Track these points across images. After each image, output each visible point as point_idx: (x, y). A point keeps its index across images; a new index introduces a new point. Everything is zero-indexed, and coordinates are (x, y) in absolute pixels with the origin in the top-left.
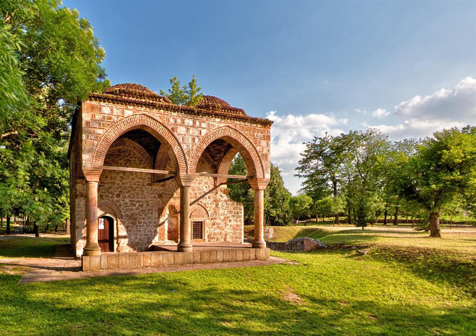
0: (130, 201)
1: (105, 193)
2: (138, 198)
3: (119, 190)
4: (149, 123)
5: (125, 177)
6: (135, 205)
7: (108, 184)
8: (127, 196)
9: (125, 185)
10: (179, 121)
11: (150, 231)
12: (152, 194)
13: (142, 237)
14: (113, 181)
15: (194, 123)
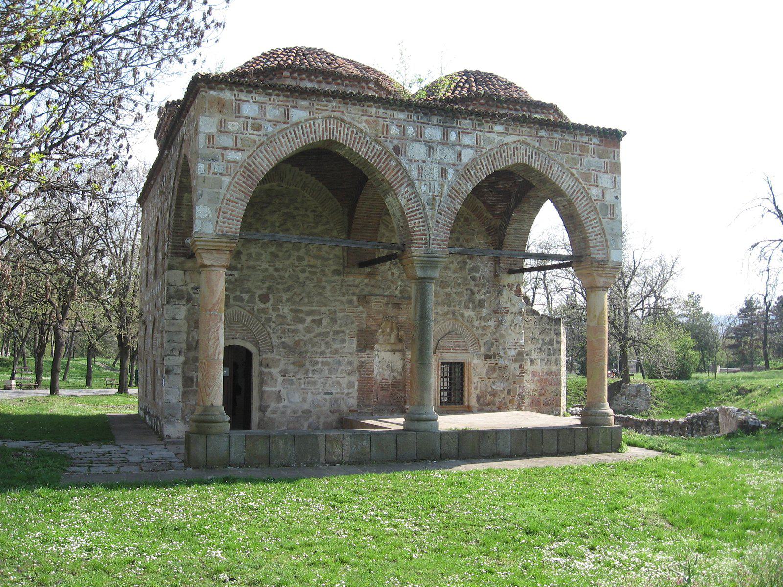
0: (291, 310)
2: (310, 303)
3: (267, 284)
4: (342, 135)
5: (281, 254)
6: (302, 321)
8: (285, 299)
9: (282, 273)
10: (410, 131)
11: (339, 383)
12: (344, 295)
13: (319, 397)
14: (251, 263)
15: (446, 136)
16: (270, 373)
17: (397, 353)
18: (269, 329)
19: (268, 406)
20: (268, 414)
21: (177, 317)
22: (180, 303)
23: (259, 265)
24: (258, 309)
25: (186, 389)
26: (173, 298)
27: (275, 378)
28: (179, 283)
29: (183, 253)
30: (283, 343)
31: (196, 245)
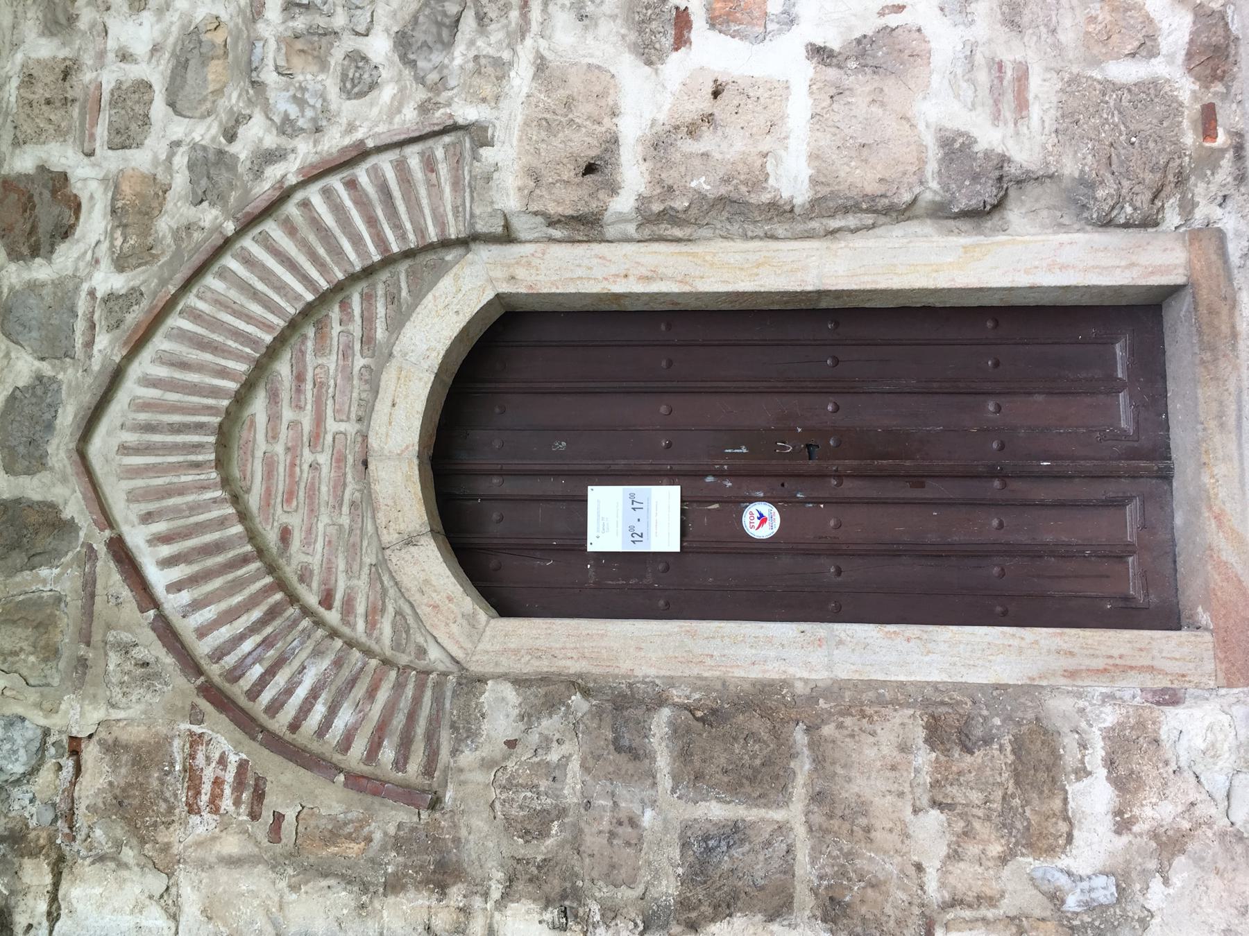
8: (44, 49)
16: (658, 147)
18: (288, 171)
19: (955, 149)
20: (1024, 144)
24: (121, 263)
25: (804, 899)
27: (703, 103)
30: (403, 42)
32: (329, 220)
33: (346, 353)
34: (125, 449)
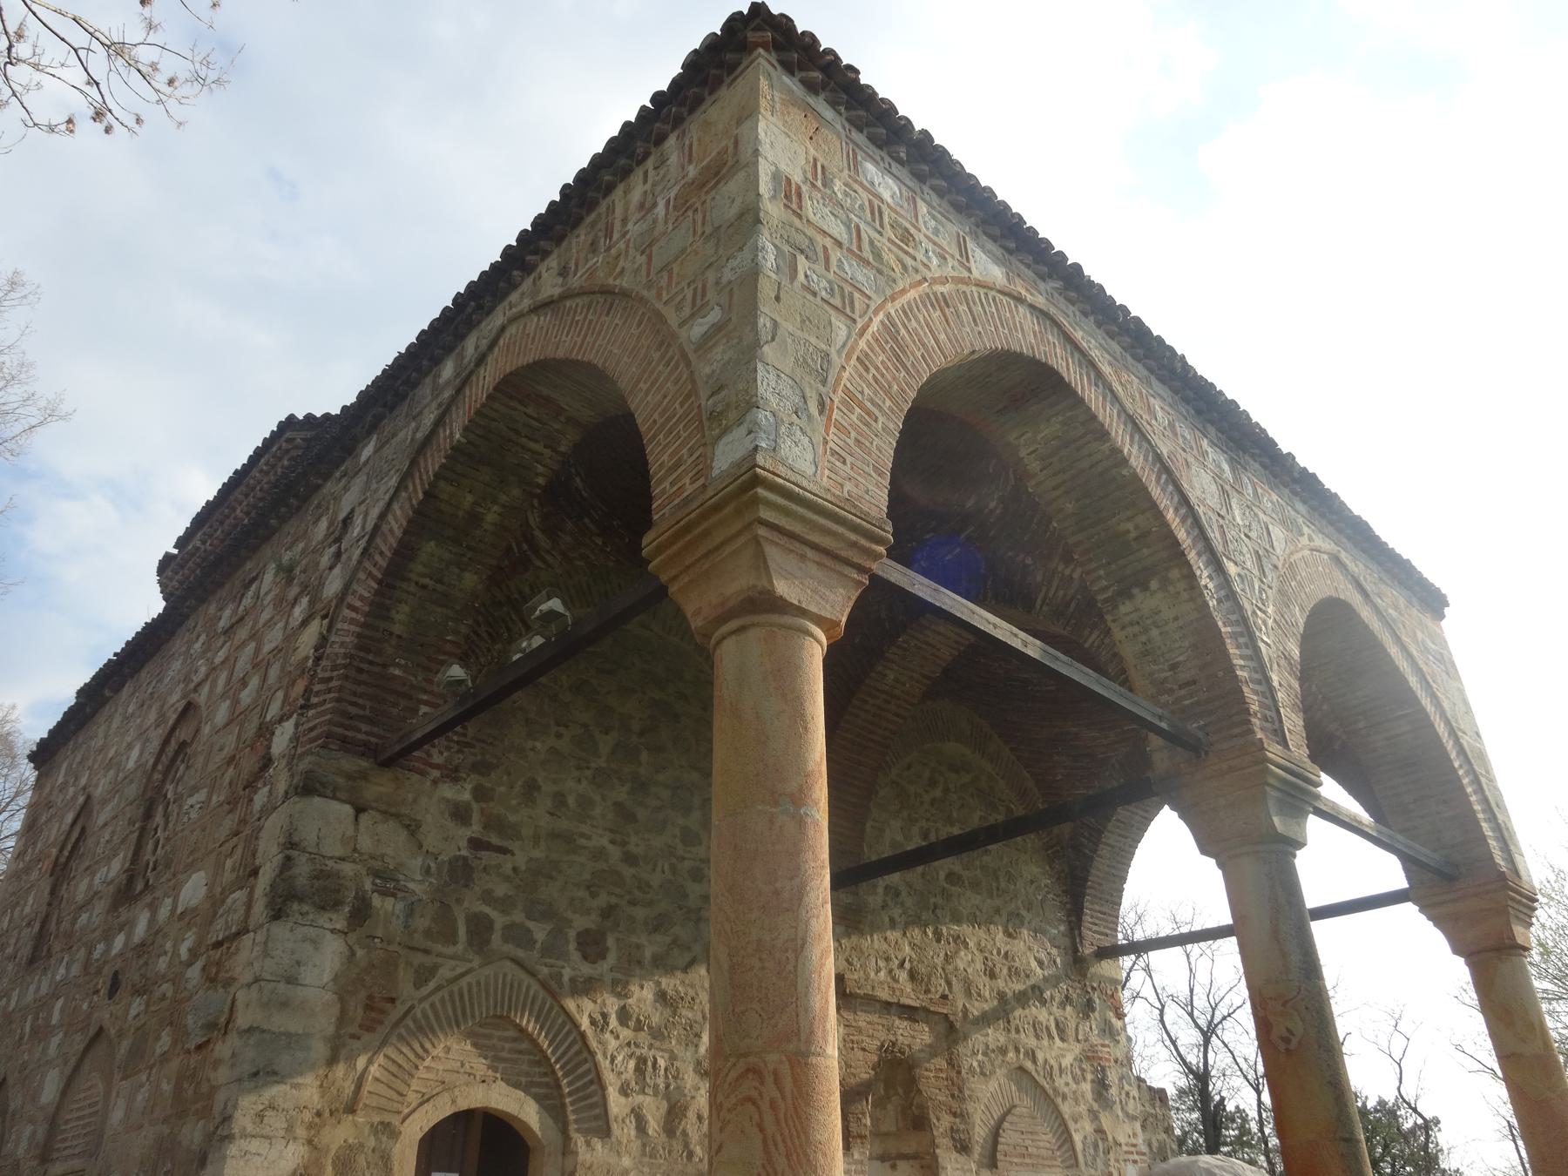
1: (505, 904)
3: (603, 900)
5: (642, 814)
7: (536, 840)
8: (648, 954)
14: (564, 824)
17: (902, 1165)
21: (309, 975)
22: (323, 920)
23: (583, 835)
24: (572, 980)
26: (301, 900)
28: (333, 848)
29: (365, 744)
31: (756, 501)
32: (580, 1071)
33: (527, 1074)
34: (505, 975)
